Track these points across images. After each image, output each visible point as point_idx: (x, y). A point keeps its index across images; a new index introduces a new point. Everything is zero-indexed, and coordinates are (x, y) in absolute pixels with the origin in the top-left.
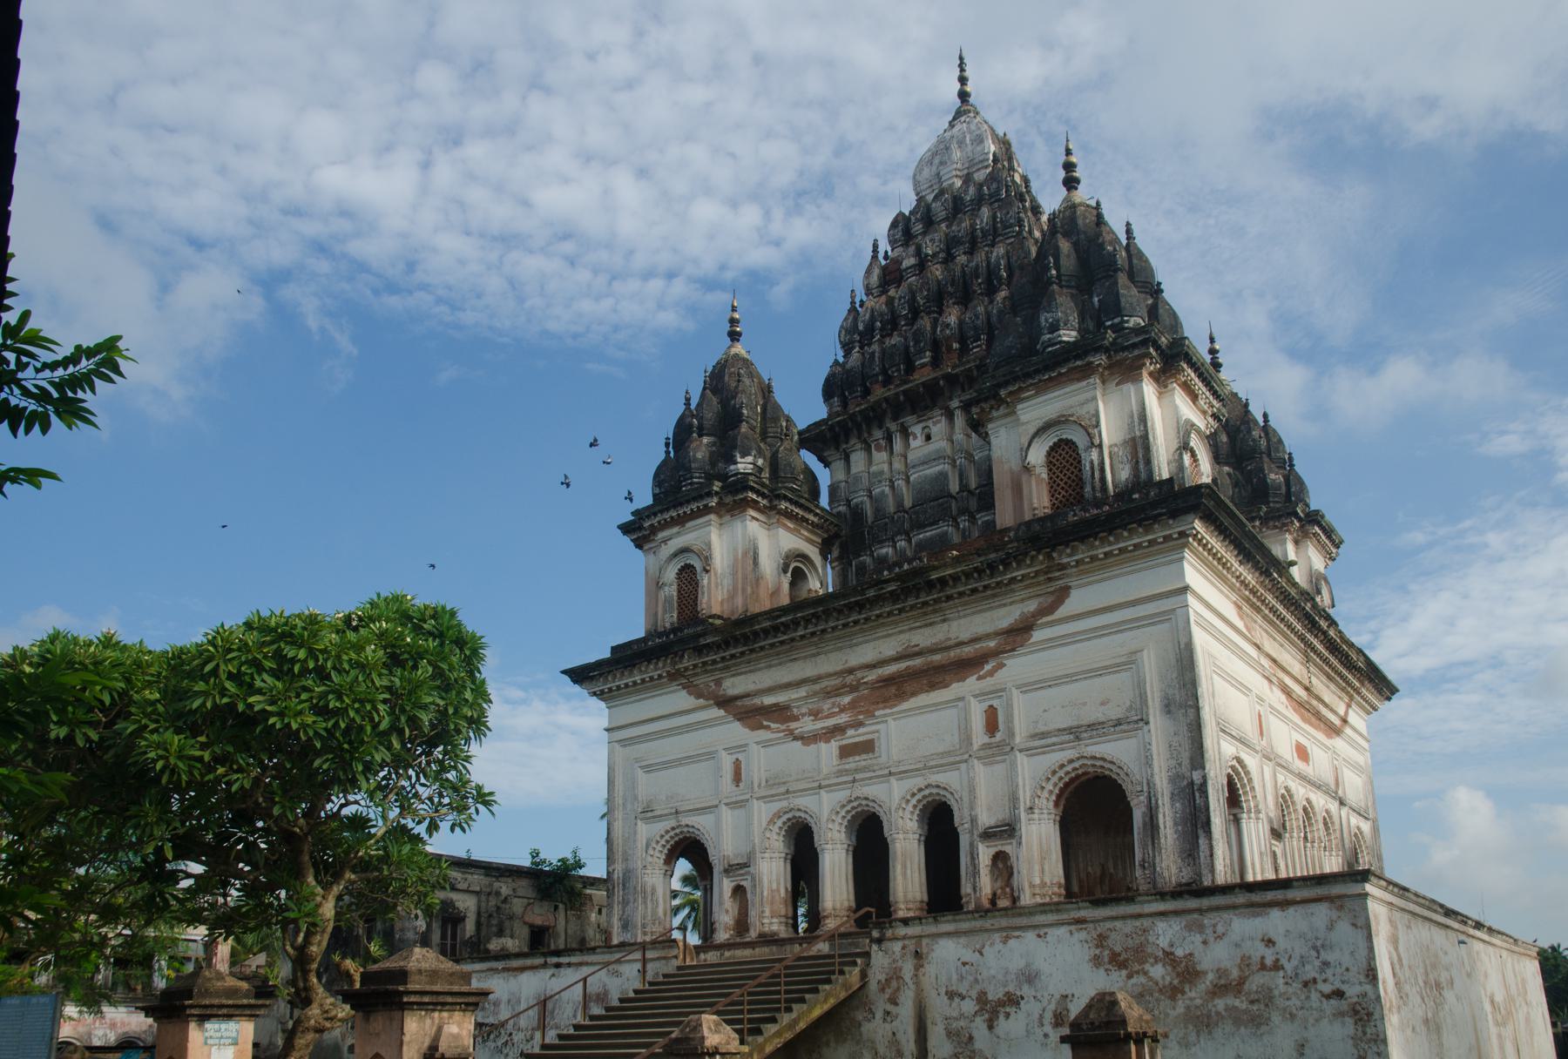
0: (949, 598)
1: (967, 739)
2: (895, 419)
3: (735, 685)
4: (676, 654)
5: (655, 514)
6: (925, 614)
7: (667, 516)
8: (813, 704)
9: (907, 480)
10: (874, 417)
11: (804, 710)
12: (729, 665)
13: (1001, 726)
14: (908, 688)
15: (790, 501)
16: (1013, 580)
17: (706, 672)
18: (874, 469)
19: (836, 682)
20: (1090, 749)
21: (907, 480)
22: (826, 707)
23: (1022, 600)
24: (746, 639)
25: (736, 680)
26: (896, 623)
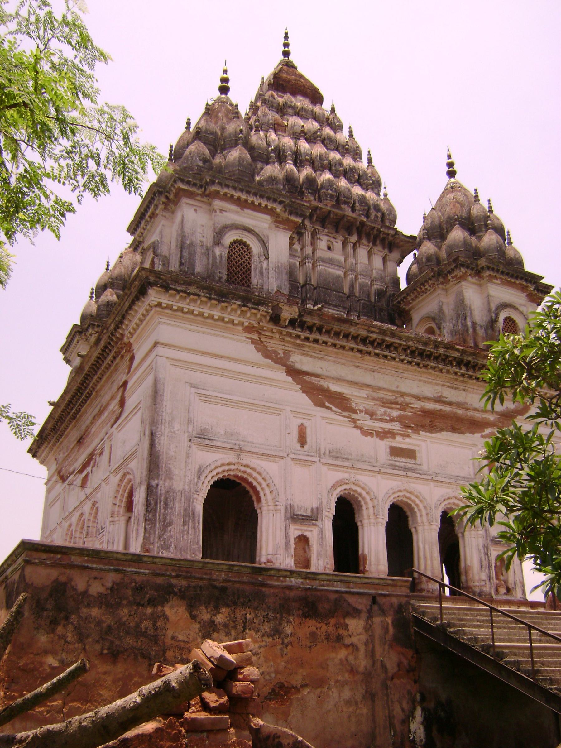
5: (227, 186)
6: (457, 380)
7: (236, 194)
8: (370, 405)
11: (361, 408)
22: (379, 412)
25: (305, 359)
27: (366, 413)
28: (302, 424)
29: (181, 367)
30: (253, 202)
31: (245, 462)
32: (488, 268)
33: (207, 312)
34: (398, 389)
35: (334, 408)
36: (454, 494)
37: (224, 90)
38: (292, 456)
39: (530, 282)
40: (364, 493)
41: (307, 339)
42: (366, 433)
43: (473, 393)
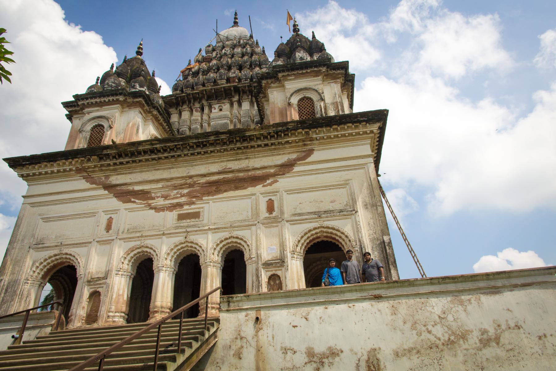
0: (252, 147)
1: (258, 214)
2: (207, 100)
3: (116, 179)
4: (85, 157)
5: (87, 99)
6: (237, 154)
7: (93, 101)
9: (209, 124)
10: (197, 98)
11: (159, 195)
12: (116, 169)
13: (276, 209)
14: (222, 188)
15: (159, 112)
16: (287, 142)
17: (102, 170)
18: (193, 118)
19: (183, 181)
20: (325, 223)
21: (209, 124)
22: (172, 194)
23: (289, 153)
24: (133, 154)
25: (119, 177)
26: (220, 156)
27: (162, 197)
28: (111, 217)
29: (37, 206)
30: (105, 101)
31: (64, 252)
32: (280, 72)
33: (49, 170)
34: (189, 174)
35: (137, 201)
36: (230, 235)
37: (139, 53)
38: (97, 240)
39: (320, 66)
40: (152, 251)
41: (115, 164)
42: (157, 209)
43: (255, 158)
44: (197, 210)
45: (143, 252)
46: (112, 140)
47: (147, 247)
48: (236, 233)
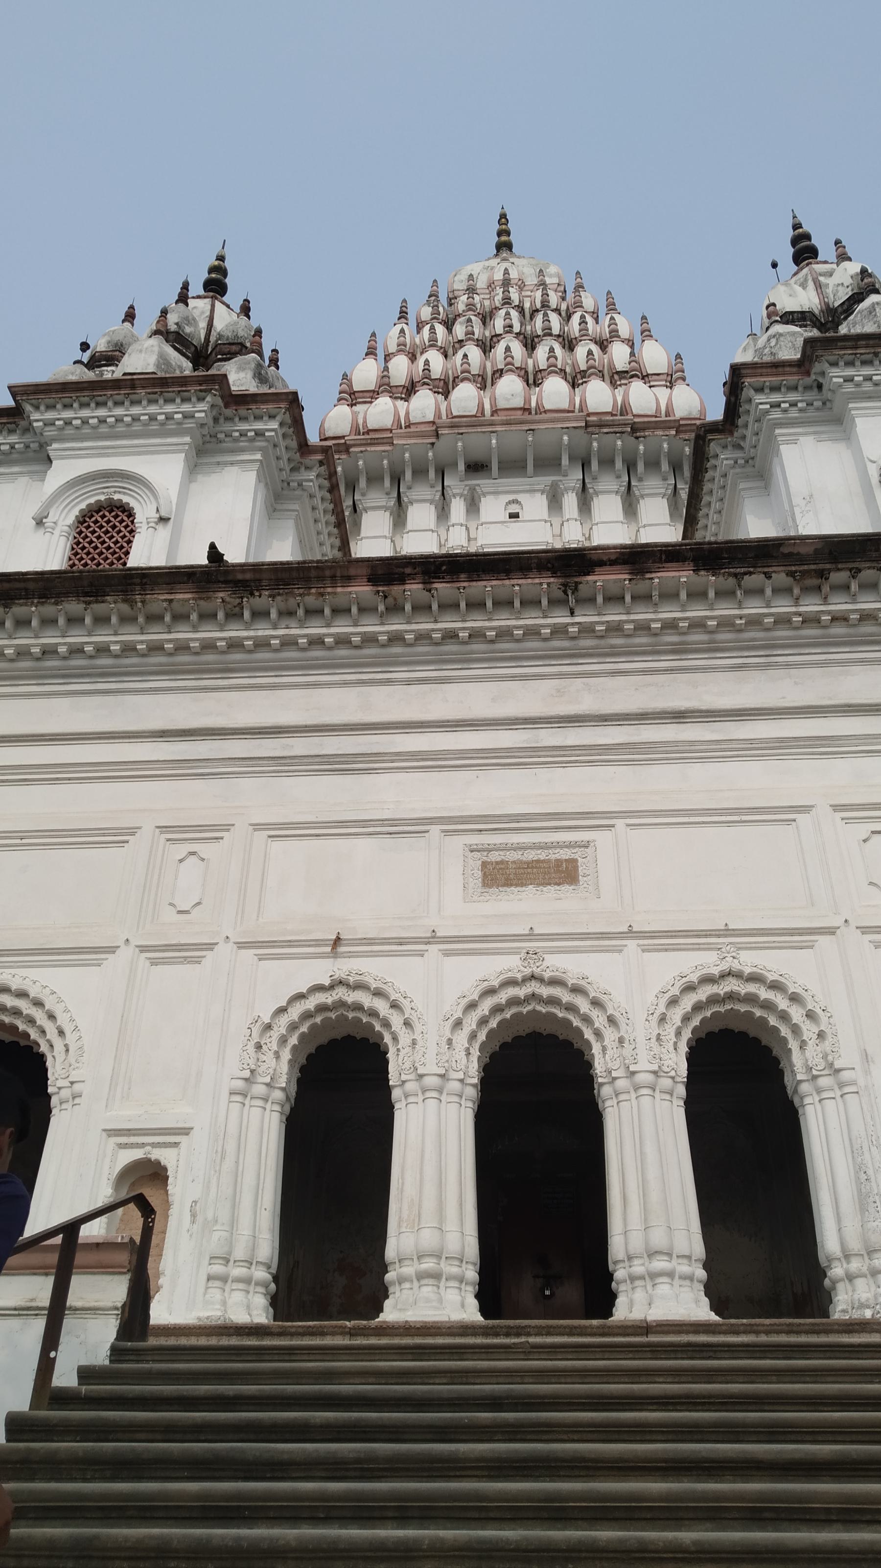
36: (724, 966)
44: (564, 854)
45: (341, 1004)
46: (213, 546)
47: (360, 986)
48: (749, 961)
